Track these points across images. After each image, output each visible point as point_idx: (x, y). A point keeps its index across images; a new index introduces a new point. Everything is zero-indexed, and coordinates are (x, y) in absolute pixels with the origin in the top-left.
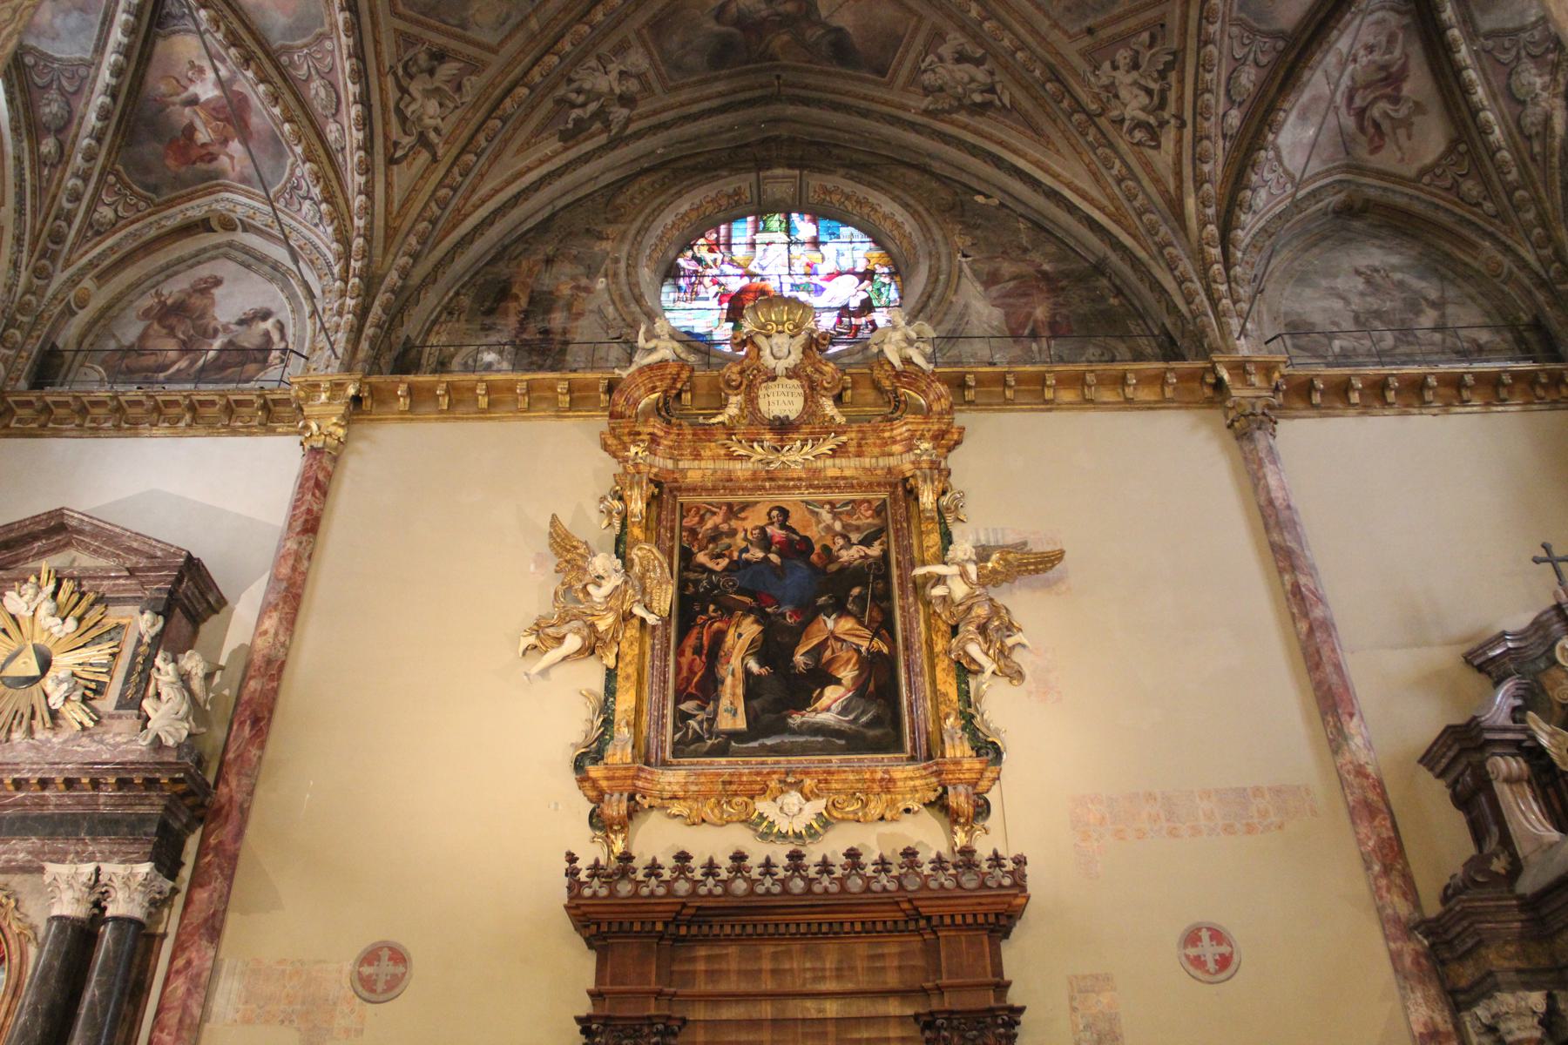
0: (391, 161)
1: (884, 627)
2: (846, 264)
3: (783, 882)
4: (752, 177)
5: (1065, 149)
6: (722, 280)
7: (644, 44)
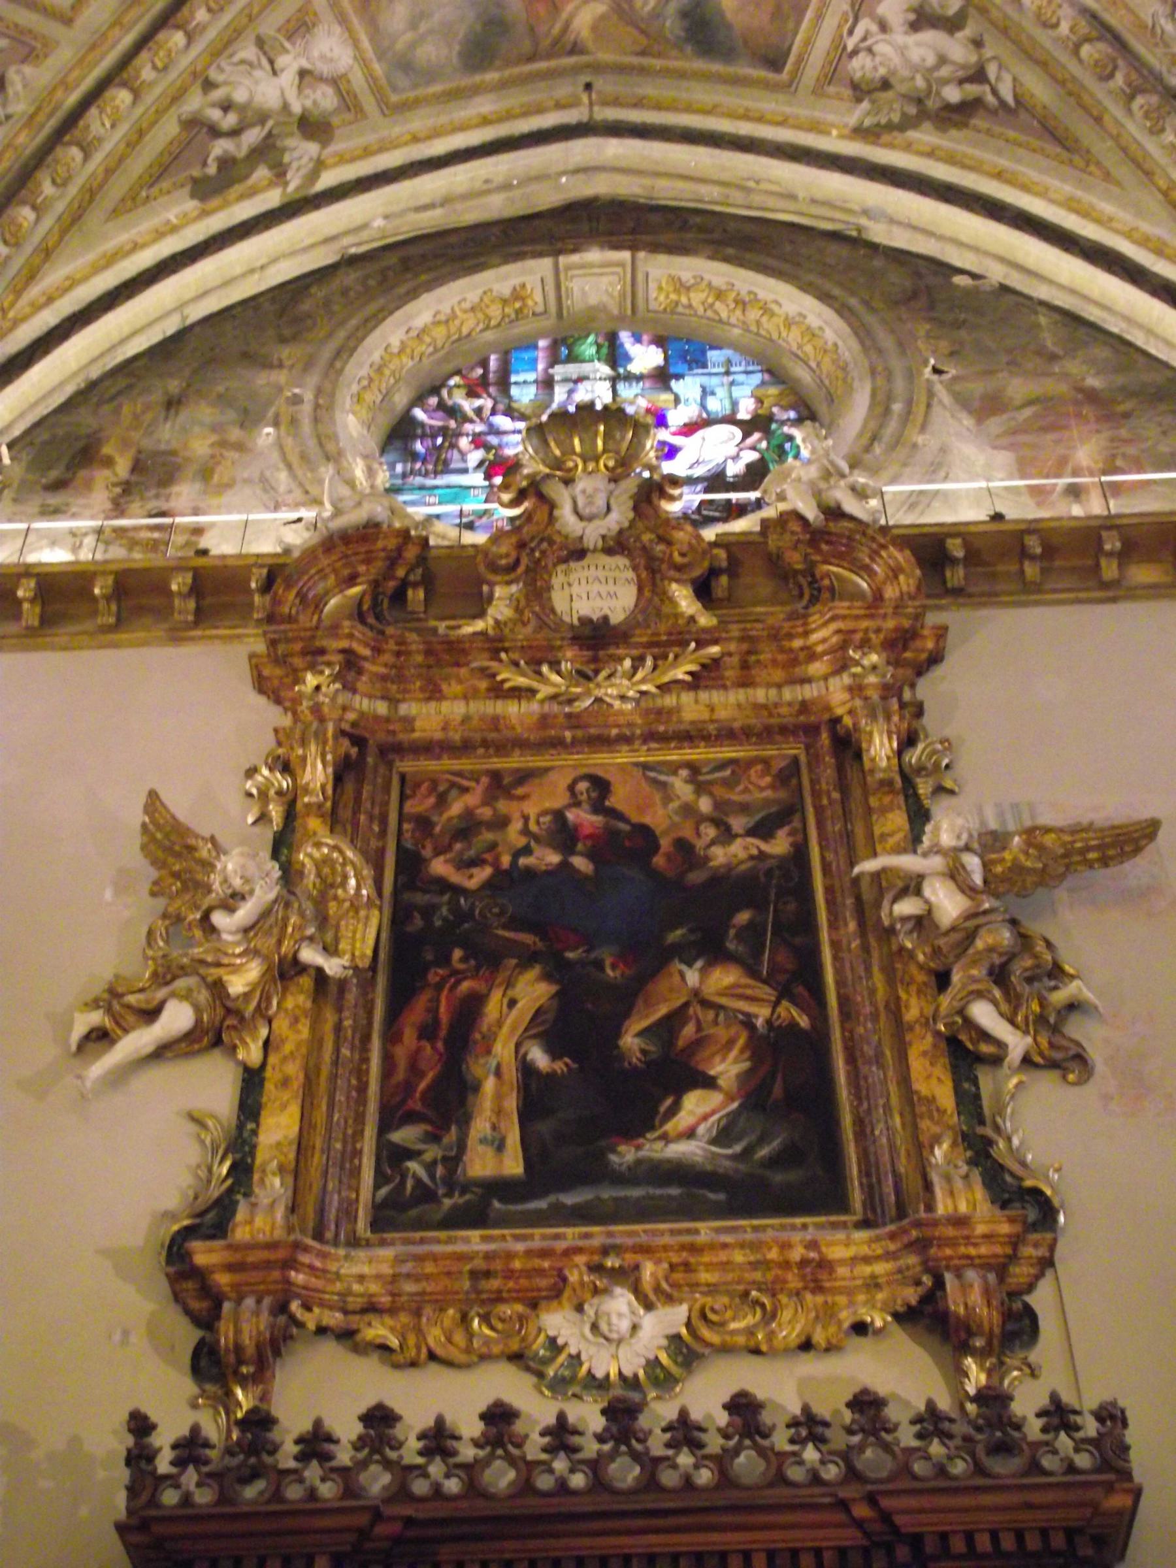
2: (716, 405)
3: (595, 1466)
4: (546, 263)
5: (1123, 172)
6: (493, 440)
7: (343, 20)
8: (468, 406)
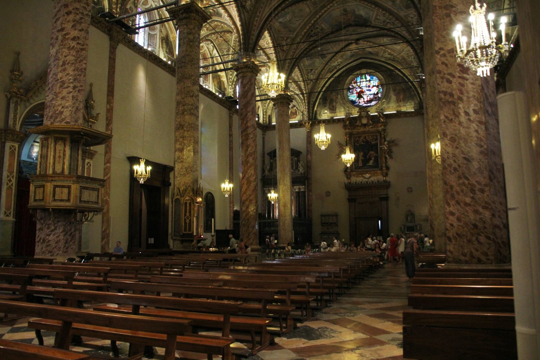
0: (308, 85)
1: (377, 153)
2: (374, 84)
8: (354, 85)
